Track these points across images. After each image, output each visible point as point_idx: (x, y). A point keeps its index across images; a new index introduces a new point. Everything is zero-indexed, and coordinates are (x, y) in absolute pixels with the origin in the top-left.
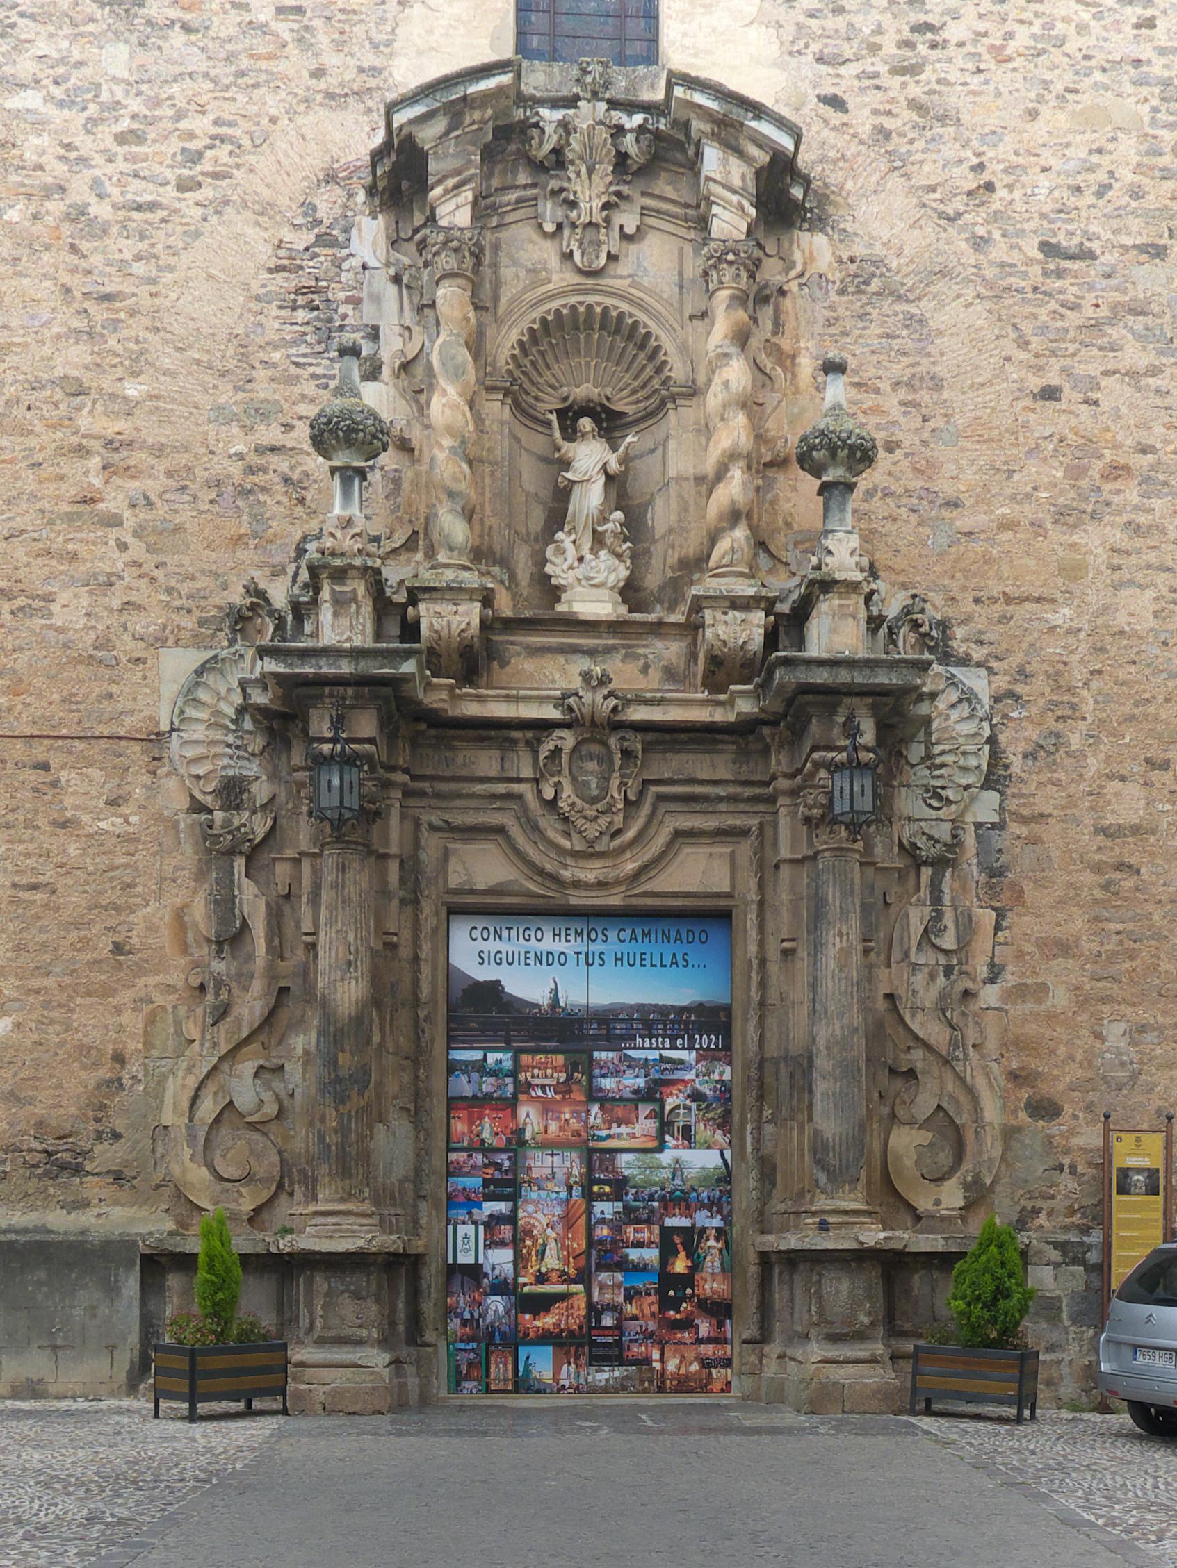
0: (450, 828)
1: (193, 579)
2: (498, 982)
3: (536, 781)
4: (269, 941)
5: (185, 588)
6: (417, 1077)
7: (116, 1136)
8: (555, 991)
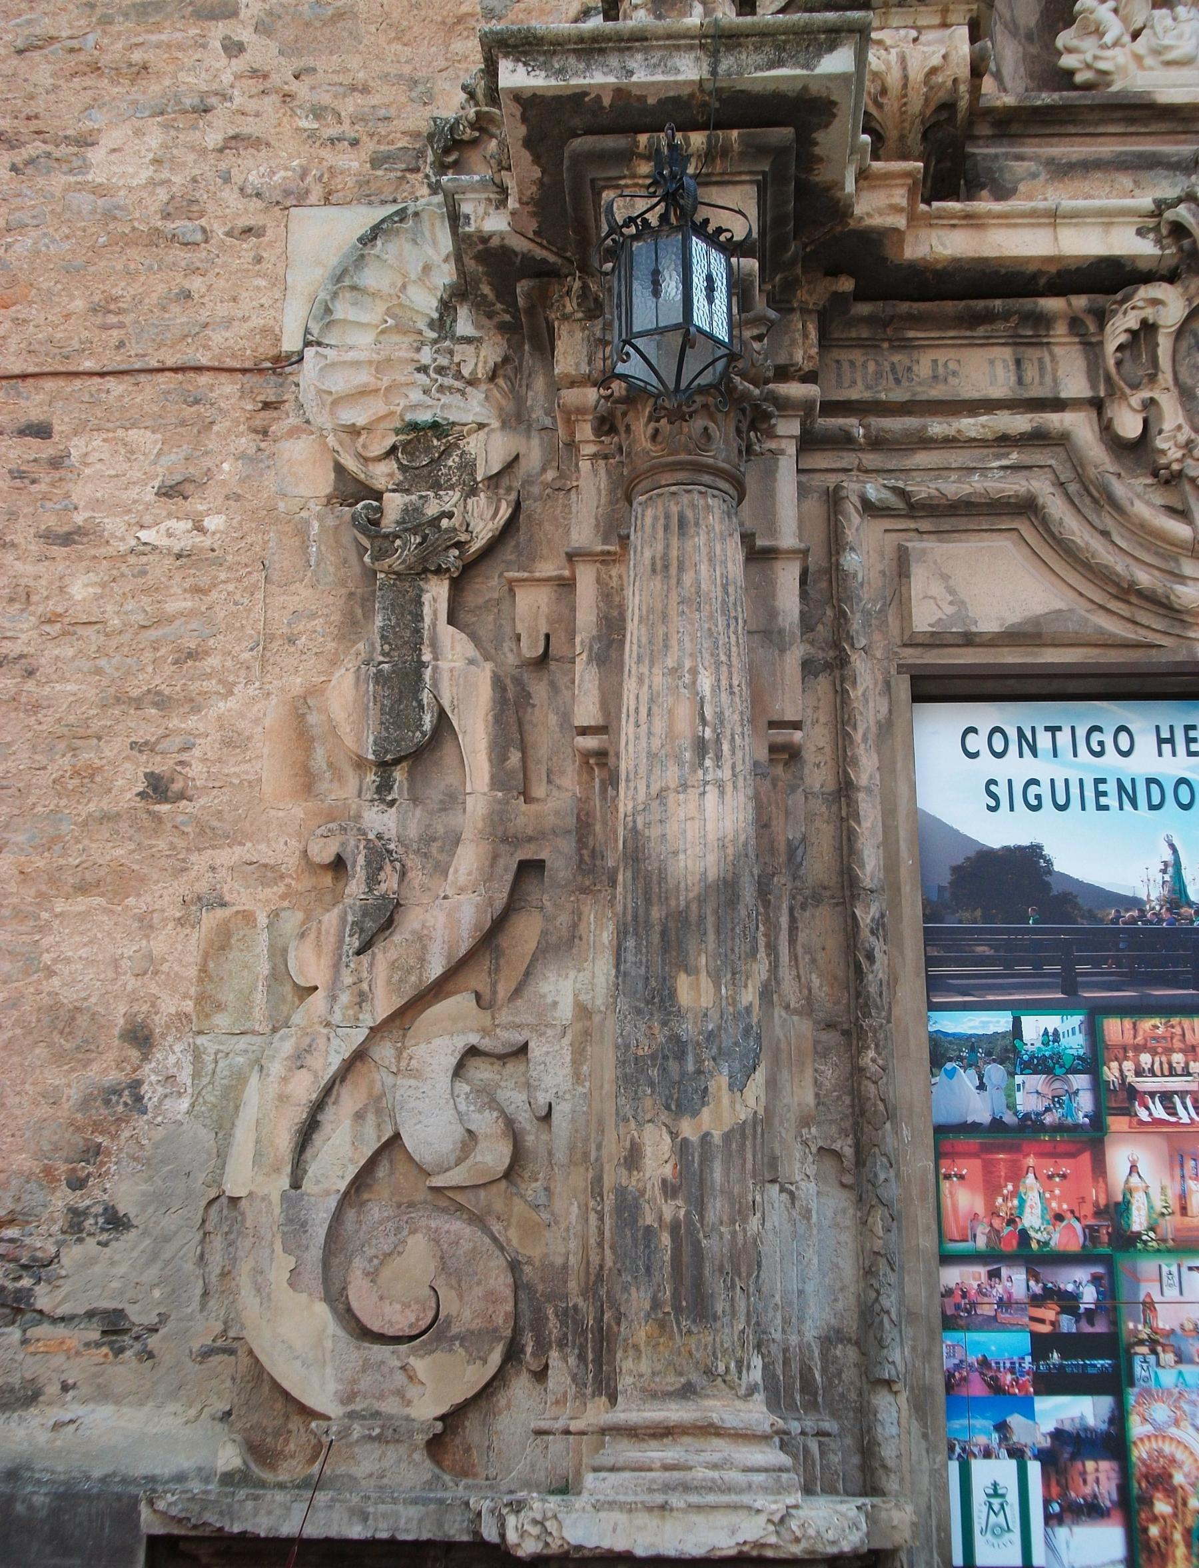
0: (914, 509)
1: (365, 90)
2: (1034, 852)
3: (1097, 405)
4: (498, 754)
5: (350, 105)
6: (858, 1072)
7: (116, 1222)
8: (1175, 867)
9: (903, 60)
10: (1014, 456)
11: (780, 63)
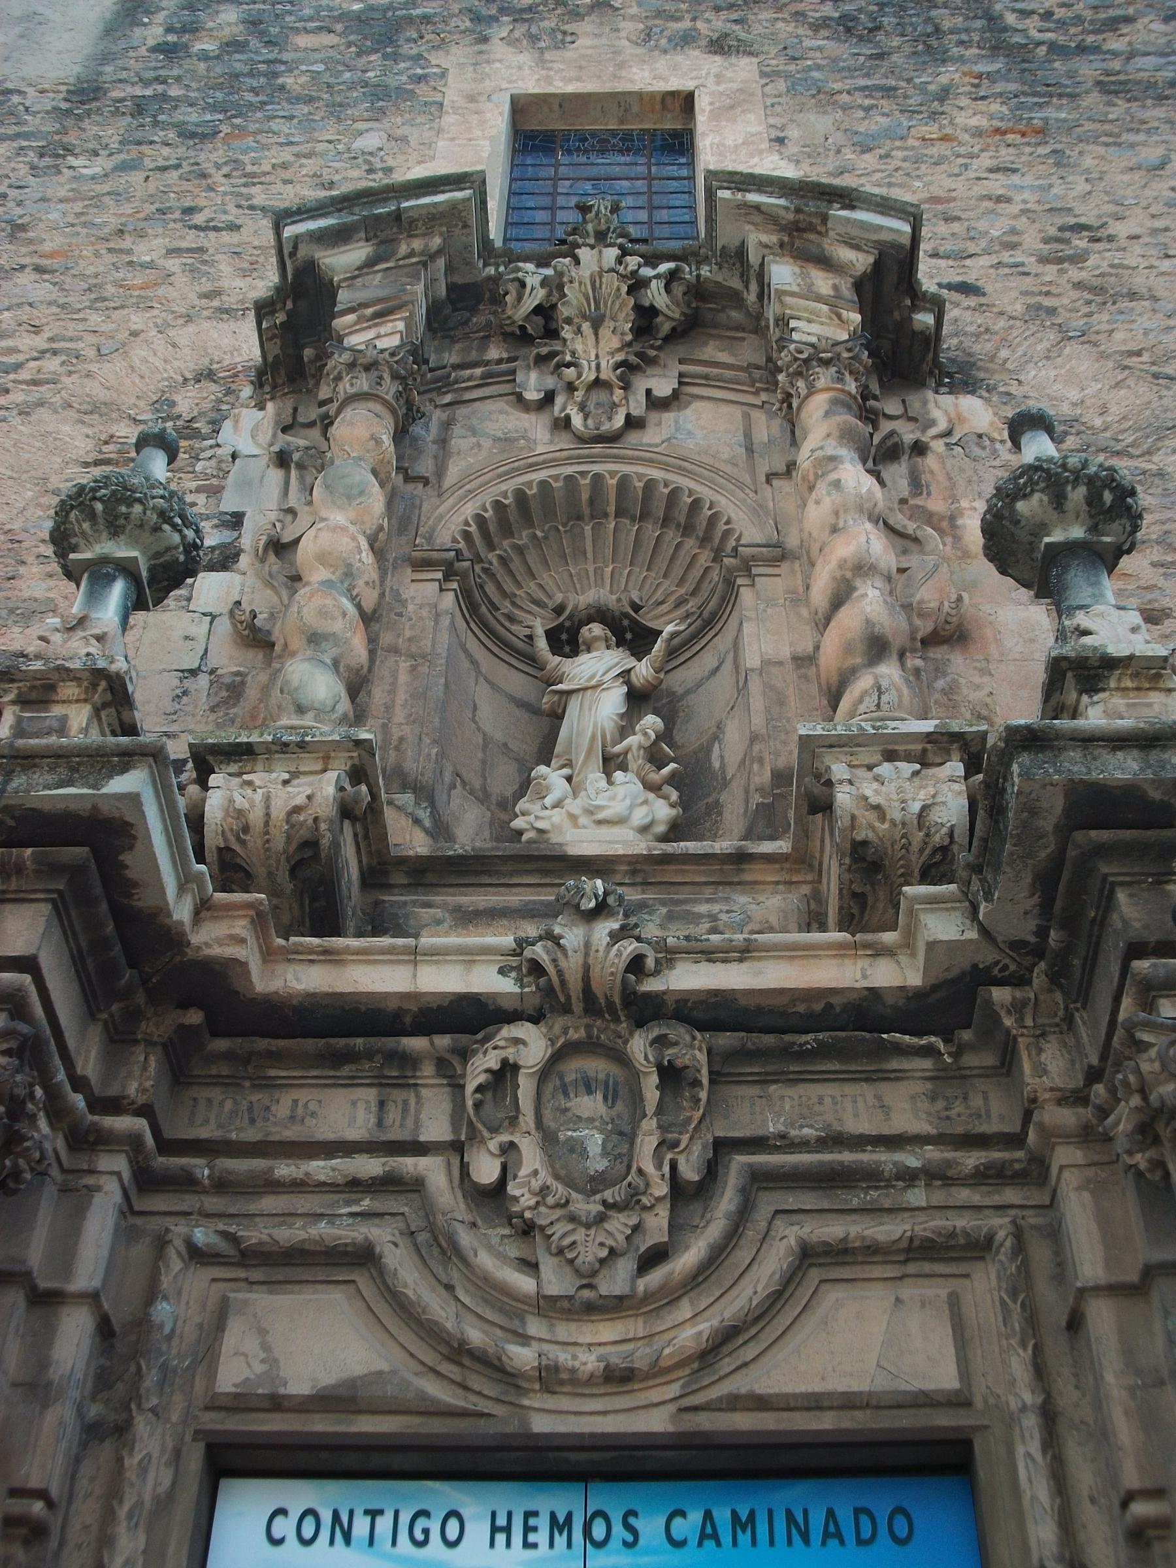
9: (267, 798)
10: (367, 1202)
11: (69, 783)
